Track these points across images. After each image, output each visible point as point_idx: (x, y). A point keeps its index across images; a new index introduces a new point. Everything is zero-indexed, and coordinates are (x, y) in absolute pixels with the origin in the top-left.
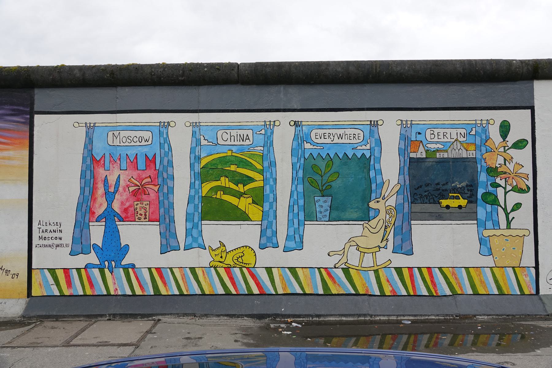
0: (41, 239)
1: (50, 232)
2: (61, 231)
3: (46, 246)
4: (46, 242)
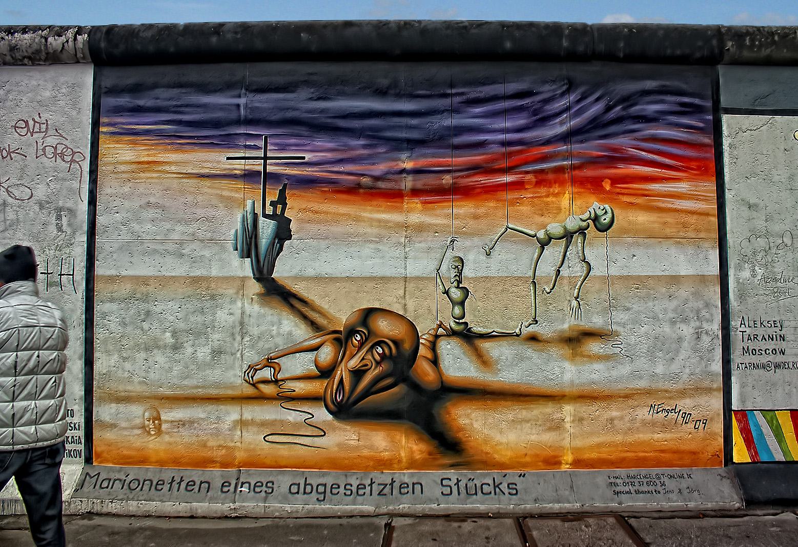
0: (746, 353)
1: (764, 340)
2: (783, 338)
3: (756, 366)
4: (755, 359)
